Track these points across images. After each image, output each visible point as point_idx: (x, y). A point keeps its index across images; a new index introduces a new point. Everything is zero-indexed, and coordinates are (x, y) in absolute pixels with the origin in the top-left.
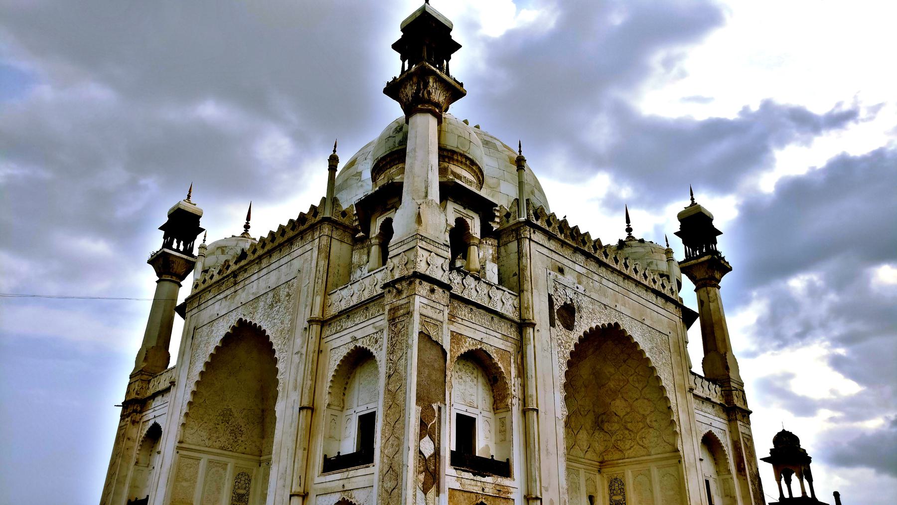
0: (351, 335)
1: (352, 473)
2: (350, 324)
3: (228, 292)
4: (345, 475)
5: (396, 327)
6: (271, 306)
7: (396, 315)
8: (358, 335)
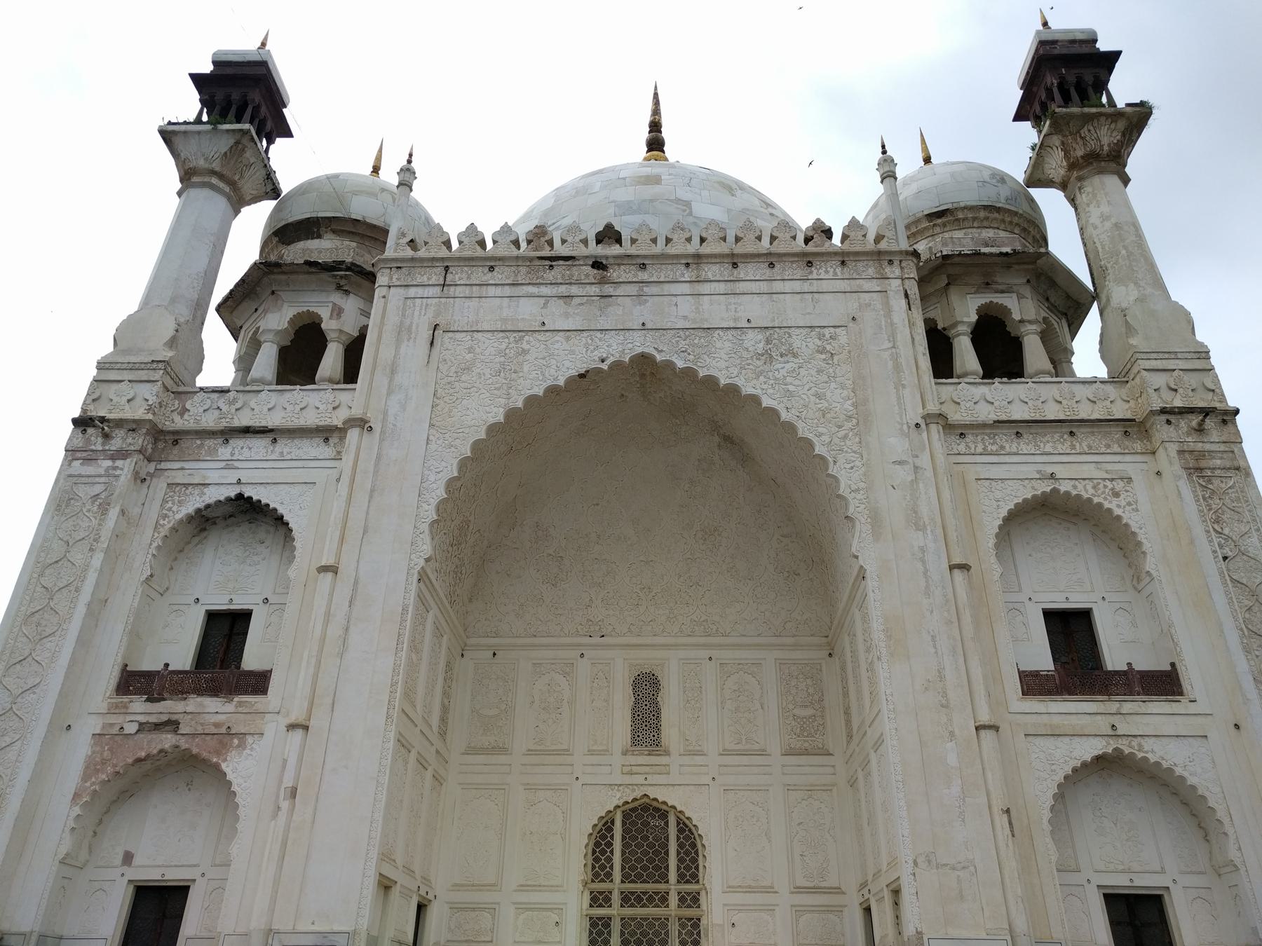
0: (1040, 467)
1: (1128, 707)
2: (1025, 448)
3: (574, 290)
4: (1113, 707)
5: (1210, 482)
6: (768, 357)
7: (1203, 464)
8: (1060, 471)
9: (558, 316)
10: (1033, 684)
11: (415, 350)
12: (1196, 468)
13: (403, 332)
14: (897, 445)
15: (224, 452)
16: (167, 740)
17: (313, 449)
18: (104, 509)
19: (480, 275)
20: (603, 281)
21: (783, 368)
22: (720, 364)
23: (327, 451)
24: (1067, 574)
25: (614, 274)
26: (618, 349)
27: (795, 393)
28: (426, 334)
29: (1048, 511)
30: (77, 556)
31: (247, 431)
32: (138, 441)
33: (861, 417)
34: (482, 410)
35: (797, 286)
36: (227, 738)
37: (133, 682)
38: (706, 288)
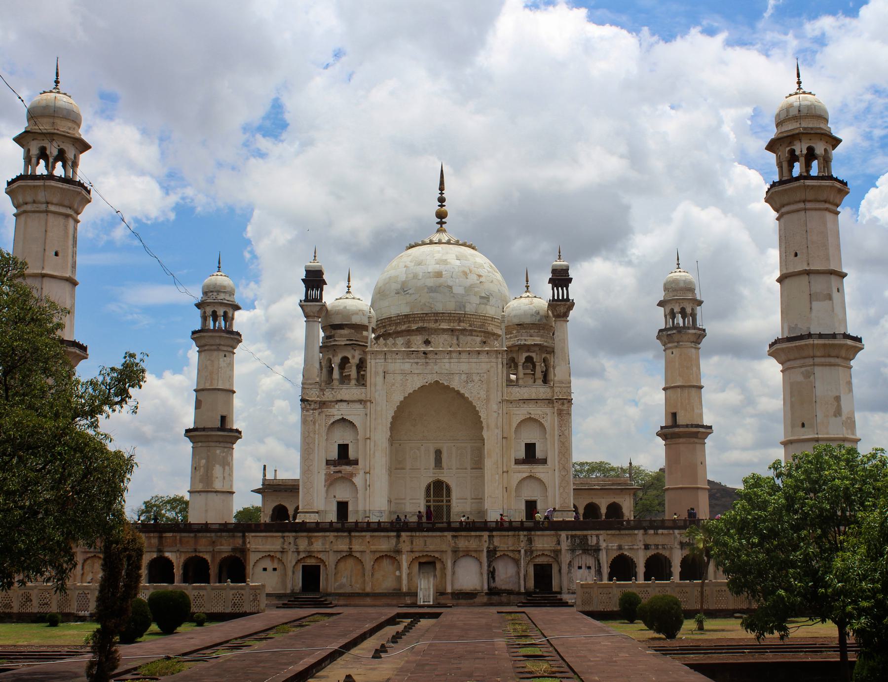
3: (419, 361)
9: (417, 369)
10: (518, 462)
11: (380, 379)
12: (560, 413)
13: (376, 373)
14: (495, 407)
15: (337, 406)
16: (340, 475)
17: (358, 406)
18: (314, 423)
19: (394, 356)
20: (426, 358)
21: (470, 385)
22: (456, 384)
23: (361, 406)
24: (531, 435)
25: (428, 356)
26: (431, 379)
27: (473, 392)
28: (382, 375)
29: (530, 420)
30: (312, 435)
31: (341, 401)
32: (317, 406)
33: (488, 400)
34: (398, 398)
35: (475, 360)
36: (352, 475)
37: (328, 462)
38: (452, 360)
